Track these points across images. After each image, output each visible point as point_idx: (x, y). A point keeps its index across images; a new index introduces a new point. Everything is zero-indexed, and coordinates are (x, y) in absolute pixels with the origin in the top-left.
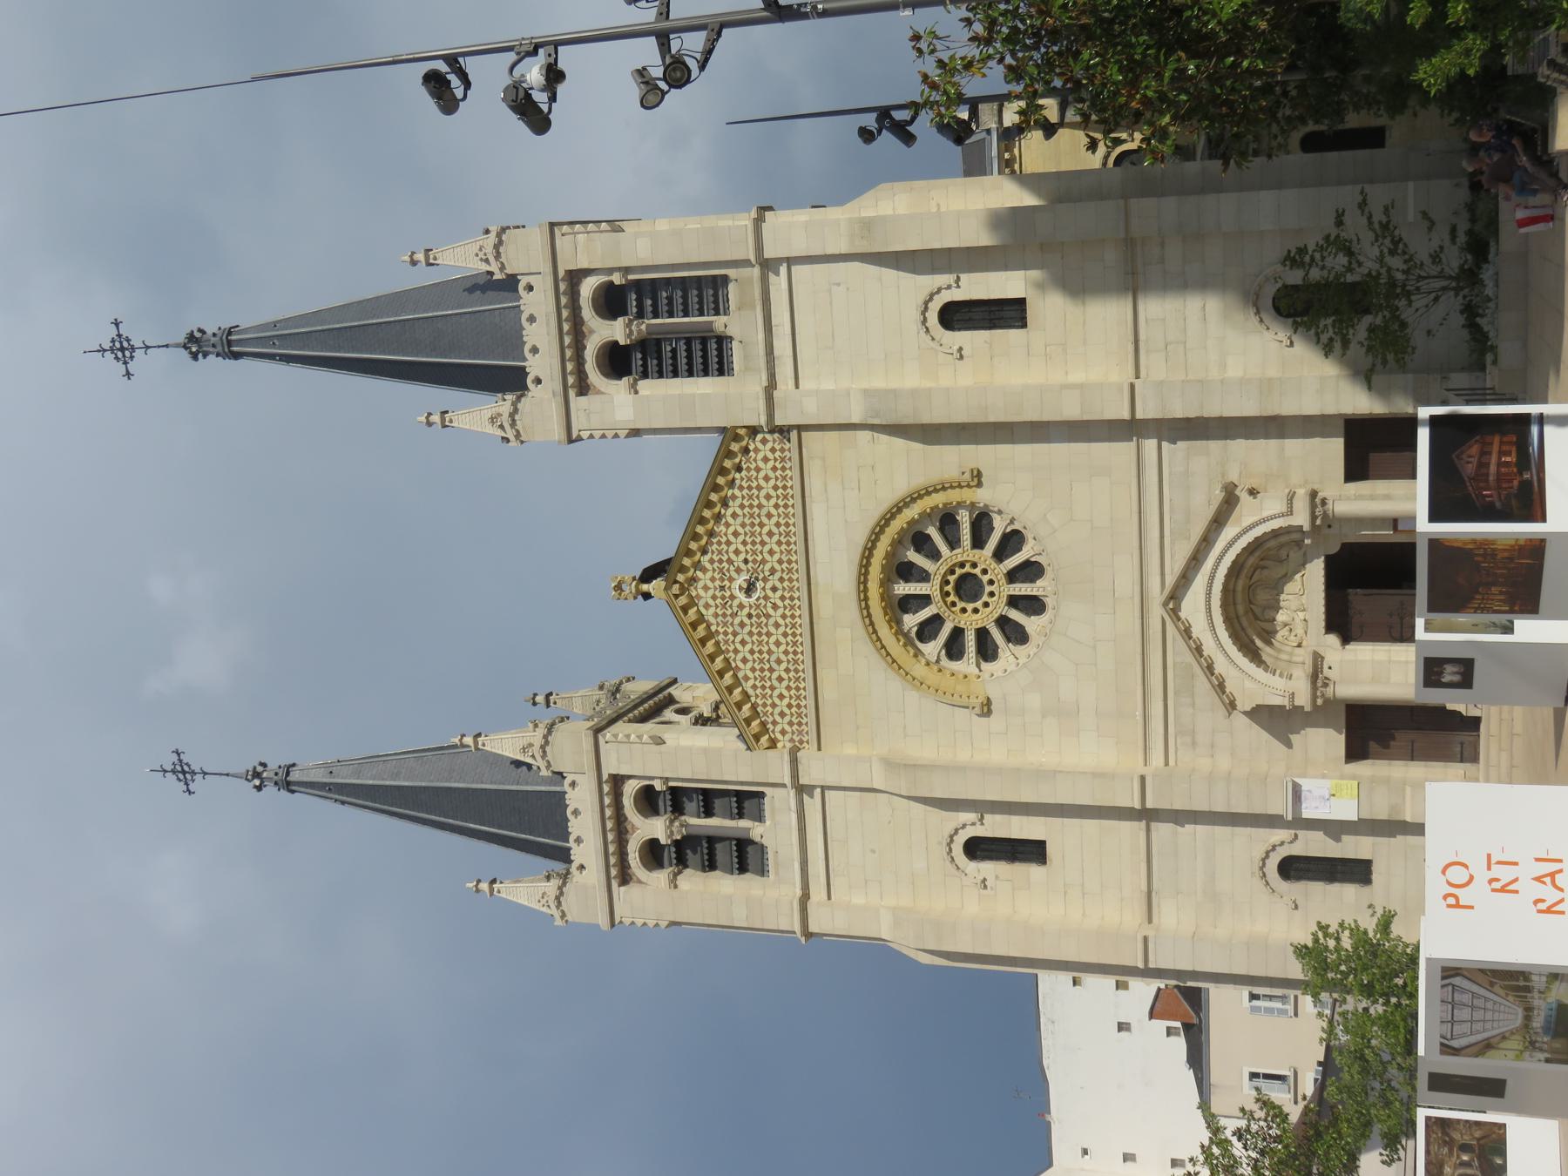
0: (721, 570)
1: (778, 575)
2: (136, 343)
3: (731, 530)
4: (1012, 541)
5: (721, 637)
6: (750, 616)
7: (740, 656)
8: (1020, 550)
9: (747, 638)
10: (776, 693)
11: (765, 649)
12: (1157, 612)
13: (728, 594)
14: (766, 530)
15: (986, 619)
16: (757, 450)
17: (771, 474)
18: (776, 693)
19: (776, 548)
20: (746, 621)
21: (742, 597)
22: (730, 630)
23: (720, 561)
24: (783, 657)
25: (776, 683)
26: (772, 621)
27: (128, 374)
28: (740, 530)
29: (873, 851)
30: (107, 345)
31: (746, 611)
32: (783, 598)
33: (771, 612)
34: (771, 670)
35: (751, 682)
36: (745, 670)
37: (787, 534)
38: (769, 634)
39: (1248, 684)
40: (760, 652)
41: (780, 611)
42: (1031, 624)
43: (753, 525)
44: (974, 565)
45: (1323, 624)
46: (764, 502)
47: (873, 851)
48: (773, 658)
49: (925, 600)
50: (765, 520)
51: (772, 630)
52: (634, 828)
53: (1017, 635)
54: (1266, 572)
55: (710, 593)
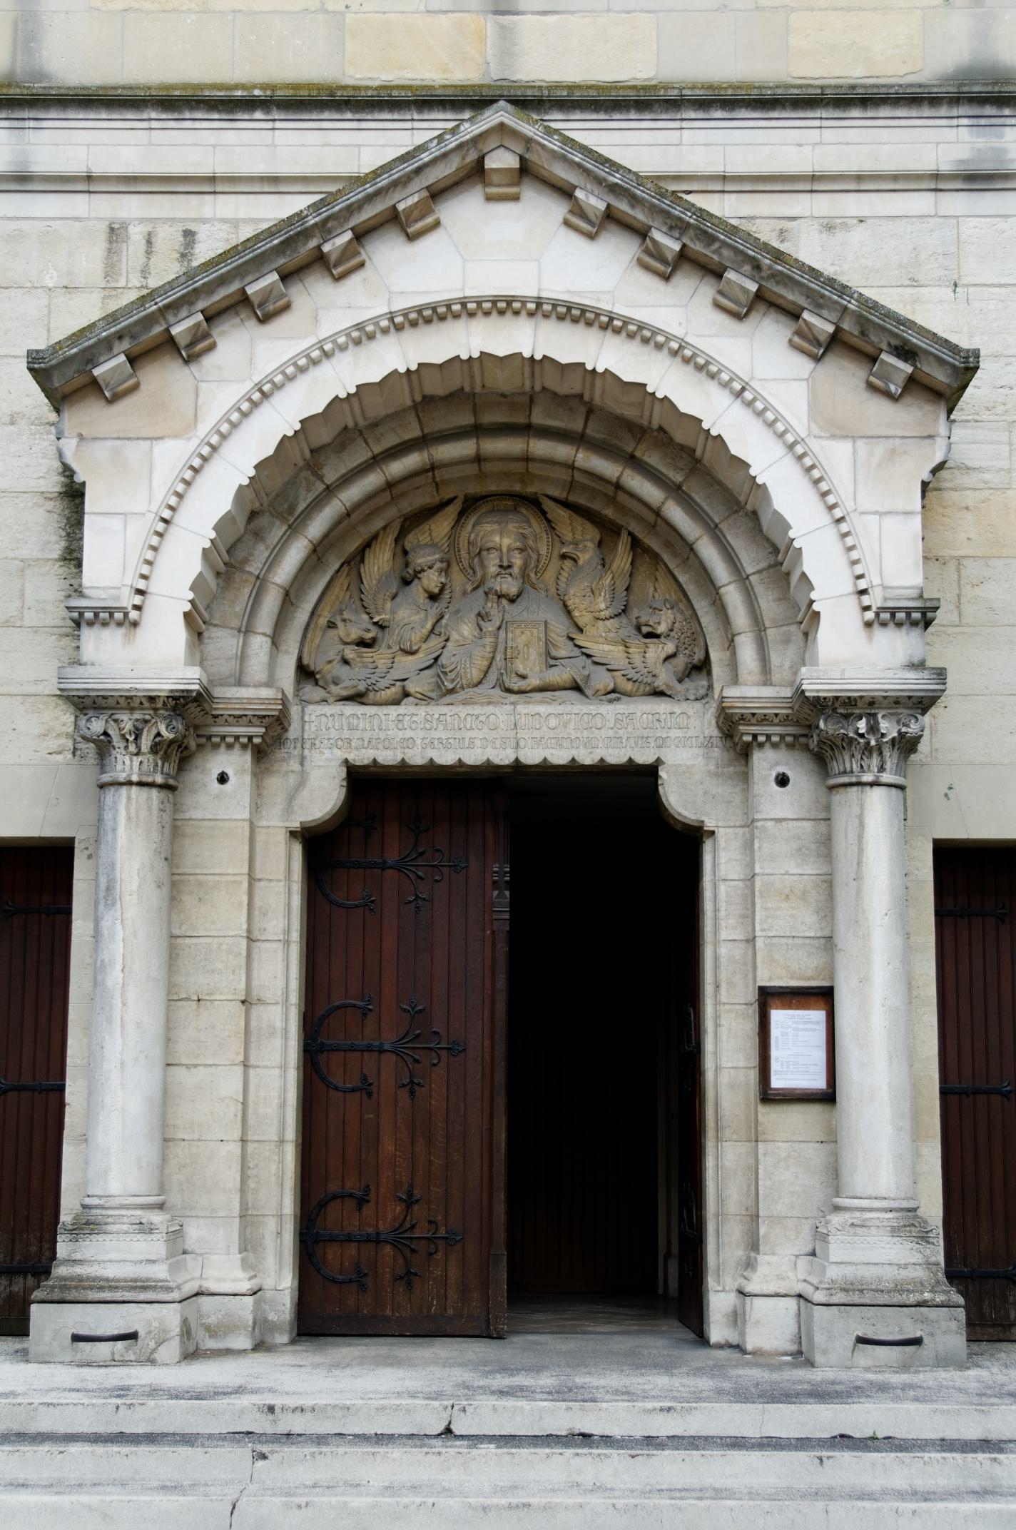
45: (388, 757)
54: (587, 555)
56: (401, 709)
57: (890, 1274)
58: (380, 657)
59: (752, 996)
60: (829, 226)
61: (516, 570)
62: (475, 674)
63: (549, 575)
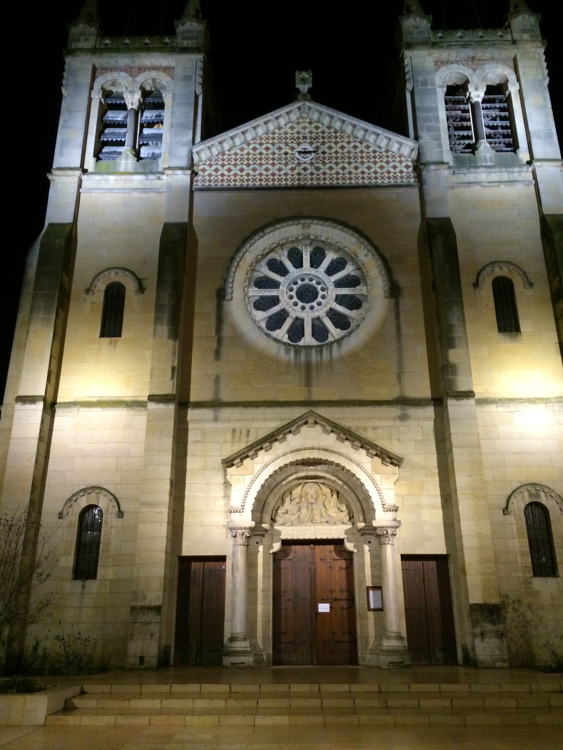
0: (317, 138)
1: (315, 172)
8: (336, 327)
11: (263, 162)
14: (346, 165)
15: (285, 303)
20: (283, 151)
22: (276, 141)
26: (283, 167)
31: (290, 151)
33: (289, 166)
38: (273, 164)
40: (261, 159)
42: (282, 334)
44: (323, 297)
50: (353, 165)
51: (277, 167)
56: (292, 527)
57: (396, 648)
58: (287, 516)
59: (365, 588)
60: (374, 428)
61: (314, 498)
62: (307, 519)
63: (321, 499)
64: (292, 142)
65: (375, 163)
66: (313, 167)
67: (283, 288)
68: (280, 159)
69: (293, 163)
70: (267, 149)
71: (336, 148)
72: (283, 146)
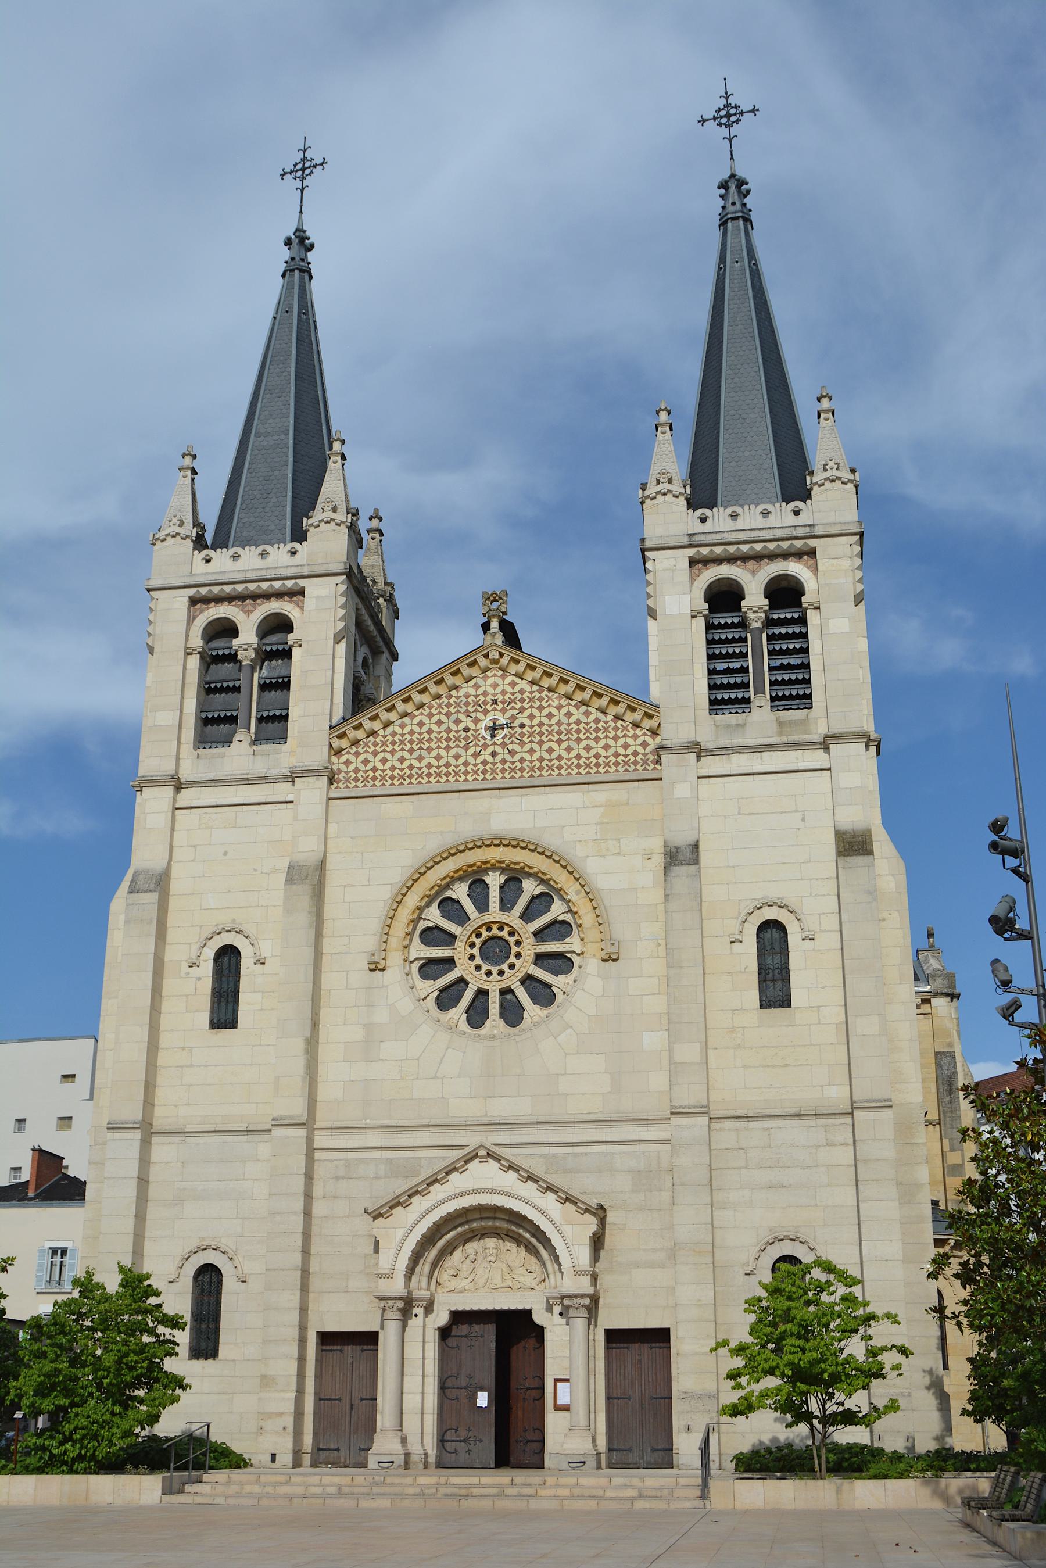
1: (508, 758)
2: (735, 129)
3: (554, 711)
4: (543, 994)
5: (445, 700)
6: (467, 730)
7: (425, 719)
9: (444, 727)
10: (388, 756)
11: (433, 745)
12: (472, 1139)
13: (489, 707)
14: (555, 746)
16: (635, 737)
17: (611, 752)
18: (388, 756)
19: (536, 756)
20: (462, 726)
21: (487, 721)
22: (452, 710)
23: (522, 700)
24: (424, 763)
25: (398, 755)
26: (462, 751)
27: (703, 121)
28: (554, 720)
29: (225, 854)
30: (732, 101)
31: (472, 726)
32: (485, 763)
33: (471, 751)
34: (411, 751)
35: (398, 730)
36: (411, 724)
37: (550, 768)
38: (448, 748)
39: (400, 1233)
40: (430, 740)
41: (471, 760)
43: (559, 733)
44: (518, 955)
45: (460, 1309)
46: (583, 744)
47: (225, 854)
48: (424, 753)
49: (482, 906)
50: (564, 745)
51: (453, 752)
52: (248, 613)
53: (446, 999)
55: (490, 690)
64: (476, 711)
65: (597, 739)
66: (506, 751)
67: (460, 944)
68: (457, 739)
69: (476, 745)
70: (439, 723)
71: (540, 717)
72: (462, 717)
